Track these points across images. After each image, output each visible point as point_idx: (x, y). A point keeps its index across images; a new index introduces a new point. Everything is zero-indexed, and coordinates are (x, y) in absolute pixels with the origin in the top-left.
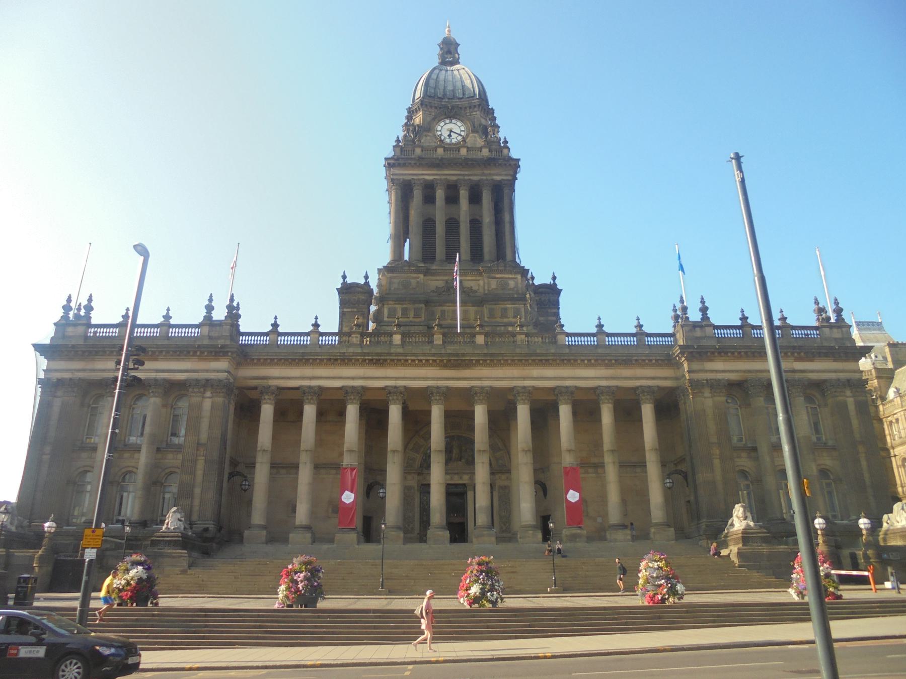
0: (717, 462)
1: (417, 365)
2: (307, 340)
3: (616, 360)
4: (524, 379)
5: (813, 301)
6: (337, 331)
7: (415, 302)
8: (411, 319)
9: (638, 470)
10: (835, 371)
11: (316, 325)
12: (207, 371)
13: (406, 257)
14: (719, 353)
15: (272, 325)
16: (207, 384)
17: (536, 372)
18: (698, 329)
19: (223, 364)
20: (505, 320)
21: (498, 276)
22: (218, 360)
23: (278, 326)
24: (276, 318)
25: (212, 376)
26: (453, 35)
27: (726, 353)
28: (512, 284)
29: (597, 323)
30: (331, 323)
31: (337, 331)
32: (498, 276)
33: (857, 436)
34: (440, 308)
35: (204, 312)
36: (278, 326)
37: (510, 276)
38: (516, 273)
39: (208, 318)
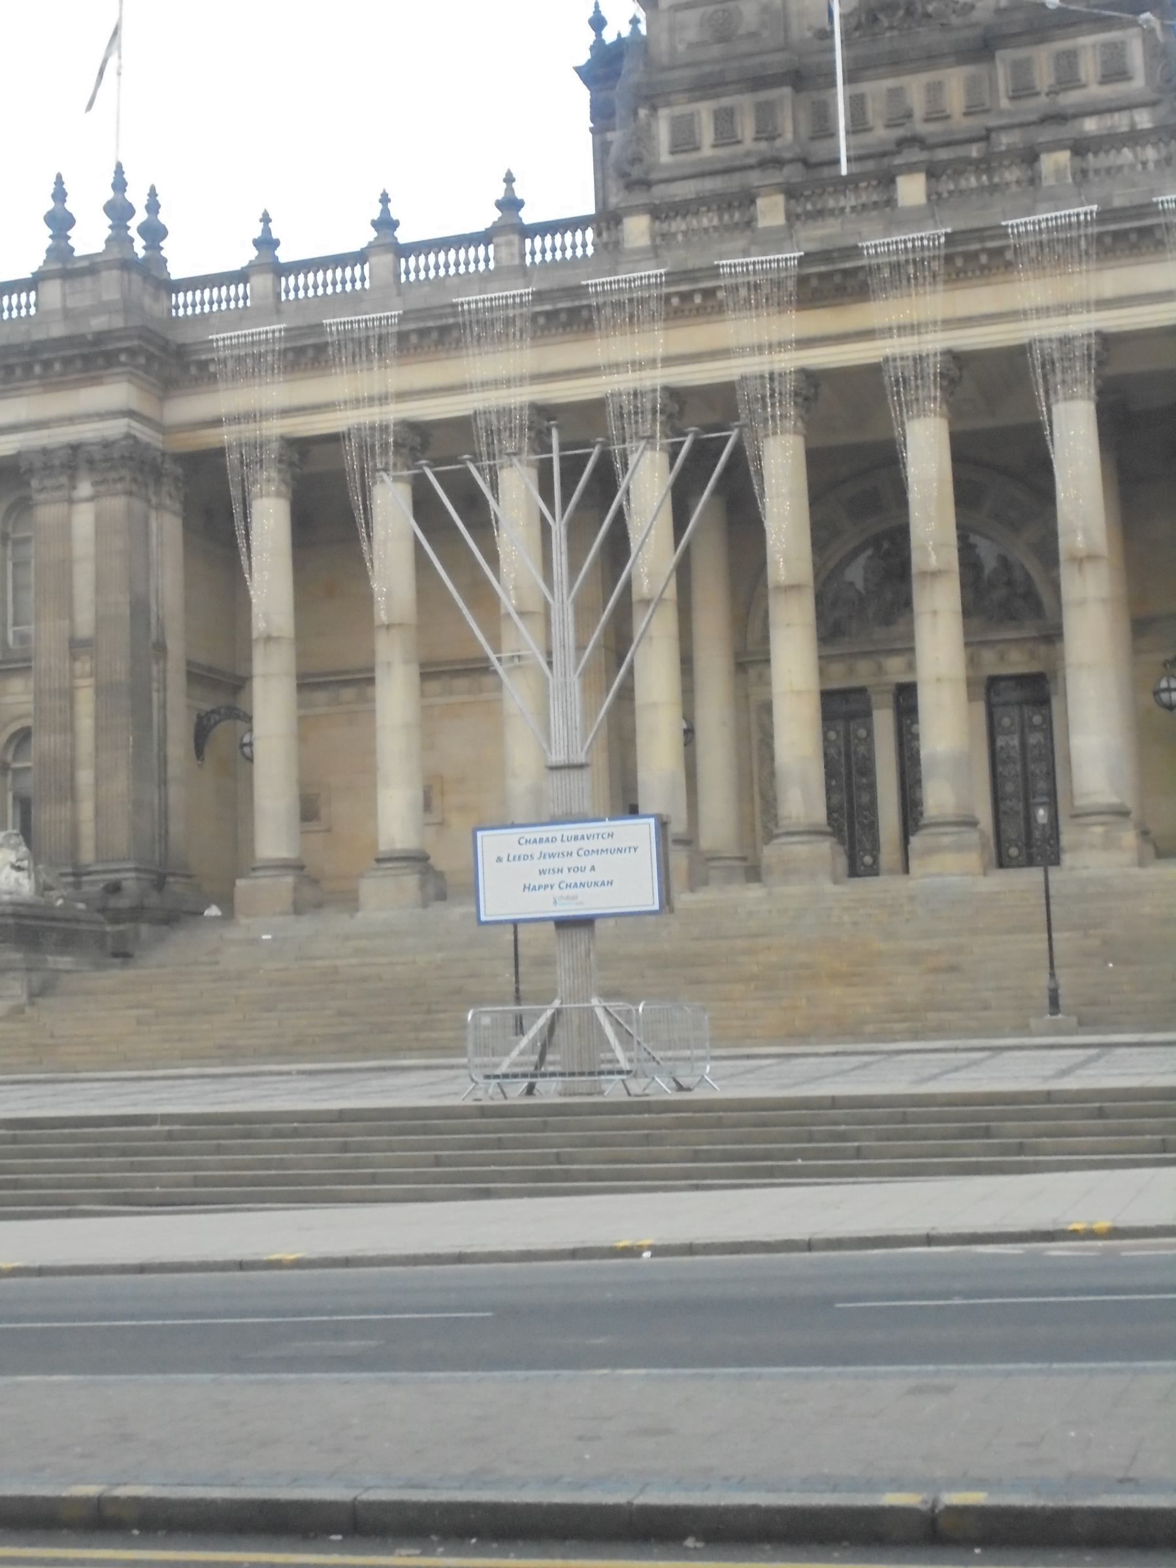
1: (700, 311)
2: (359, 276)
5: (51, 188)
6: (589, 209)
9: (348, 693)
11: (266, 243)
12: (71, 420)
15: (257, 243)
22: (96, 381)
23: (276, 243)
24: (266, 219)
25: (88, 432)
29: (500, 193)
30: (564, 184)
31: (589, 209)
36: (276, 243)
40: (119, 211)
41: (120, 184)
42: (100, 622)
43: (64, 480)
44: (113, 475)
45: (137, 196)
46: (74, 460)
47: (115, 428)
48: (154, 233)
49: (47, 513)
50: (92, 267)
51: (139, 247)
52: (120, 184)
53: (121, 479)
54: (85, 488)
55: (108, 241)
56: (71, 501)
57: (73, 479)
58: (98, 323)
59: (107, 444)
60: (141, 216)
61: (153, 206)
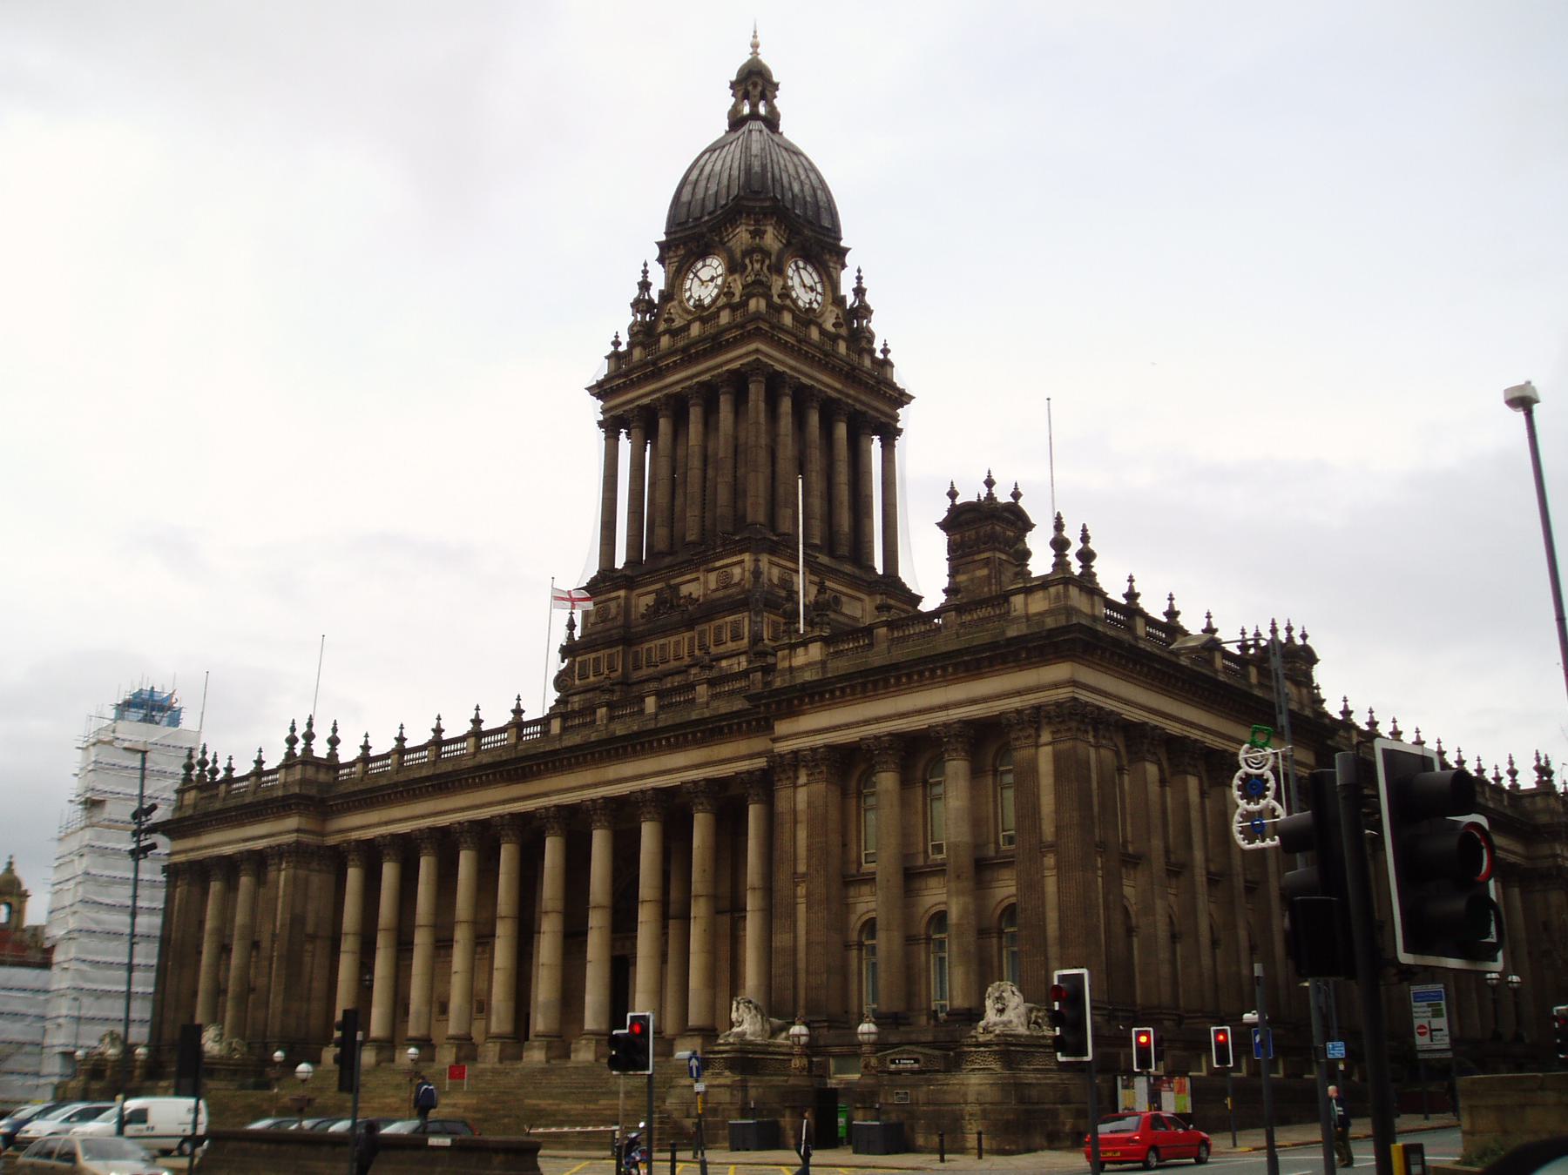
0: (802, 908)
3: (702, 732)
4: (596, 785)
7: (610, 644)
8: (592, 679)
10: (1019, 693)
13: (620, 561)
14: (811, 696)
16: (280, 853)
17: (613, 771)
18: (801, 651)
19: (292, 822)
20: (722, 649)
21: (718, 564)
26: (766, 58)
27: (822, 695)
28: (737, 571)
32: (718, 564)
33: (1048, 830)
34: (646, 646)
35: (285, 747)
37: (735, 559)
38: (741, 552)
39: (290, 754)
40: (1060, 545)
41: (1059, 526)
42: (1058, 829)
43: (1032, 732)
44: (1064, 727)
45: (1072, 534)
46: (1035, 718)
47: (1063, 694)
48: (1086, 556)
49: (1022, 755)
50: (1045, 583)
51: (1076, 568)
52: (1059, 526)
53: (1069, 729)
54: (1046, 737)
55: (1055, 565)
56: (1037, 746)
57: (1038, 730)
58: (1050, 623)
59: (1058, 705)
60: (1076, 546)
61: (1085, 538)
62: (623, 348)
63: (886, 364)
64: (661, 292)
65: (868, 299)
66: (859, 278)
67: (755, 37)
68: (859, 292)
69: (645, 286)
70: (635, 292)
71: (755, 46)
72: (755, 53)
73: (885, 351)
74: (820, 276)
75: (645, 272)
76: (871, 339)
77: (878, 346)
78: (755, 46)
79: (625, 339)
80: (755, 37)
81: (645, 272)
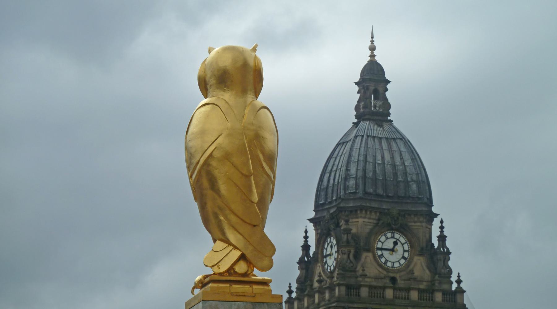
62: (294, 295)
63: (461, 291)
64: (314, 254)
65: (448, 243)
66: (442, 228)
67: (372, 41)
68: (442, 238)
69: (306, 247)
70: (300, 253)
71: (372, 49)
72: (372, 56)
73: (459, 282)
74: (405, 236)
75: (306, 237)
76: (451, 272)
77: (454, 278)
78: (372, 49)
79: (294, 288)
80: (372, 41)
81: (306, 237)
